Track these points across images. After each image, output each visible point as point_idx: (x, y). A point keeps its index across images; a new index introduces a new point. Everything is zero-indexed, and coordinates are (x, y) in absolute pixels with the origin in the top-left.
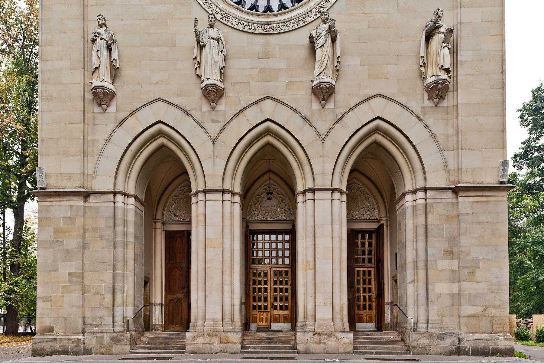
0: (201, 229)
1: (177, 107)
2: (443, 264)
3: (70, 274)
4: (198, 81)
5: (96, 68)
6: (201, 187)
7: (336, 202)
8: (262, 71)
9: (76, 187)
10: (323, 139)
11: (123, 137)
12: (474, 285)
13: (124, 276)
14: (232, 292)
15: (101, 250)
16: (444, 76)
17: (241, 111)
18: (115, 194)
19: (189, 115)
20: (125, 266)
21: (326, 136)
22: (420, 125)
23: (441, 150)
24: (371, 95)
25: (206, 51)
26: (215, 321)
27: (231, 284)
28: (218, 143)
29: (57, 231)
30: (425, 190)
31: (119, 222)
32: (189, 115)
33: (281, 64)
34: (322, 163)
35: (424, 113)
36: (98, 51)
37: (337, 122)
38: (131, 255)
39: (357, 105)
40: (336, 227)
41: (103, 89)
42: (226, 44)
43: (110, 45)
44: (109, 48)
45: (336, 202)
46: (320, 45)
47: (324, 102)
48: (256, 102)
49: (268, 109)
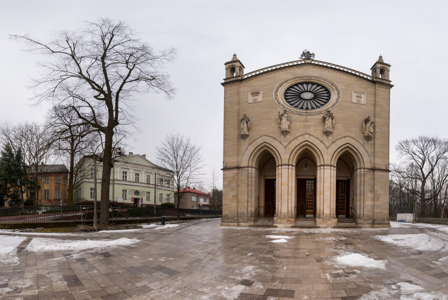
0: (280, 179)
1: (271, 137)
3: (233, 196)
4: (279, 129)
6: (280, 163)
7: (332, 170)
8: (304, 126)
11: (251, 148)
12: (378, 202)
14: (292, 203)
15: (243, 188)
18: (248, 167)
20: (252, 193)
27: (291, 199)
31: (250, 177)
33: (312, 124)
37: (333, 143)
38: (253, 189)
39: (340, 138)
40: (332, 179)
45: (332, 170)
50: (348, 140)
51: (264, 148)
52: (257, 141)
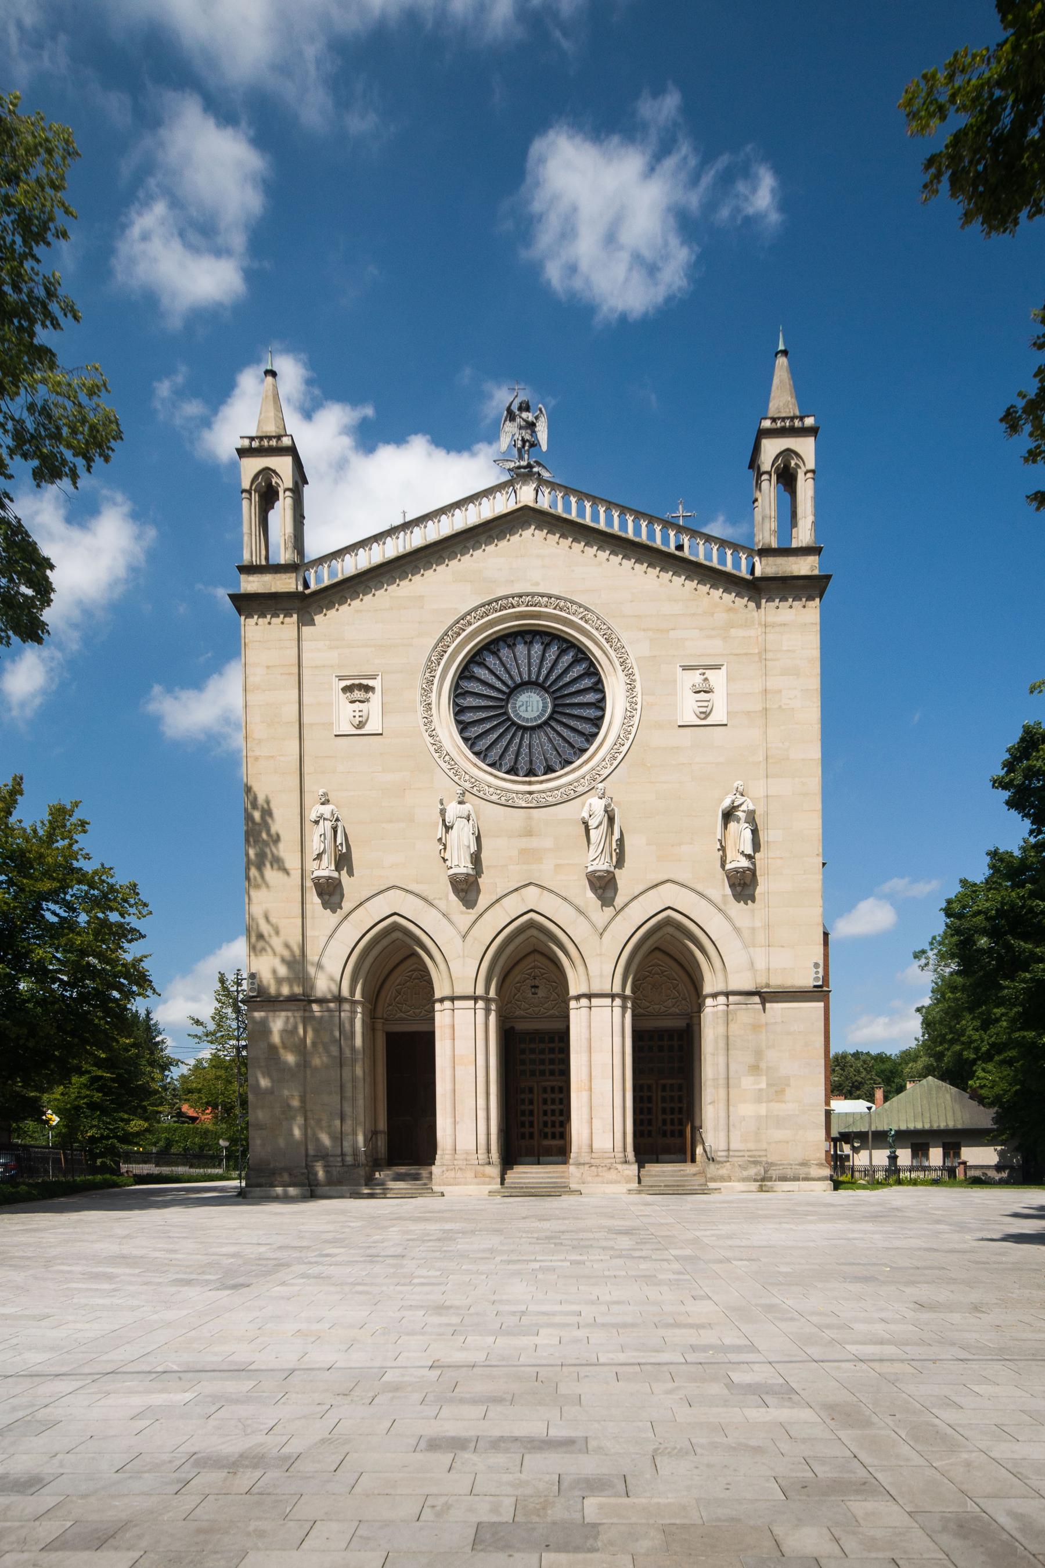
1: (417, 895)
2: (748, 1083)
8: (523, 852)
13: (354, 1099)
16: (744, 863)
17: (498, 901)
20: (354, 1087)
22: (720, 917)
23: (746, 947)
25: (453, 833)
30: (727, 994)
34: (597, 961)
35: (725, 903)
48: (516, 890)
49: (532, 898)
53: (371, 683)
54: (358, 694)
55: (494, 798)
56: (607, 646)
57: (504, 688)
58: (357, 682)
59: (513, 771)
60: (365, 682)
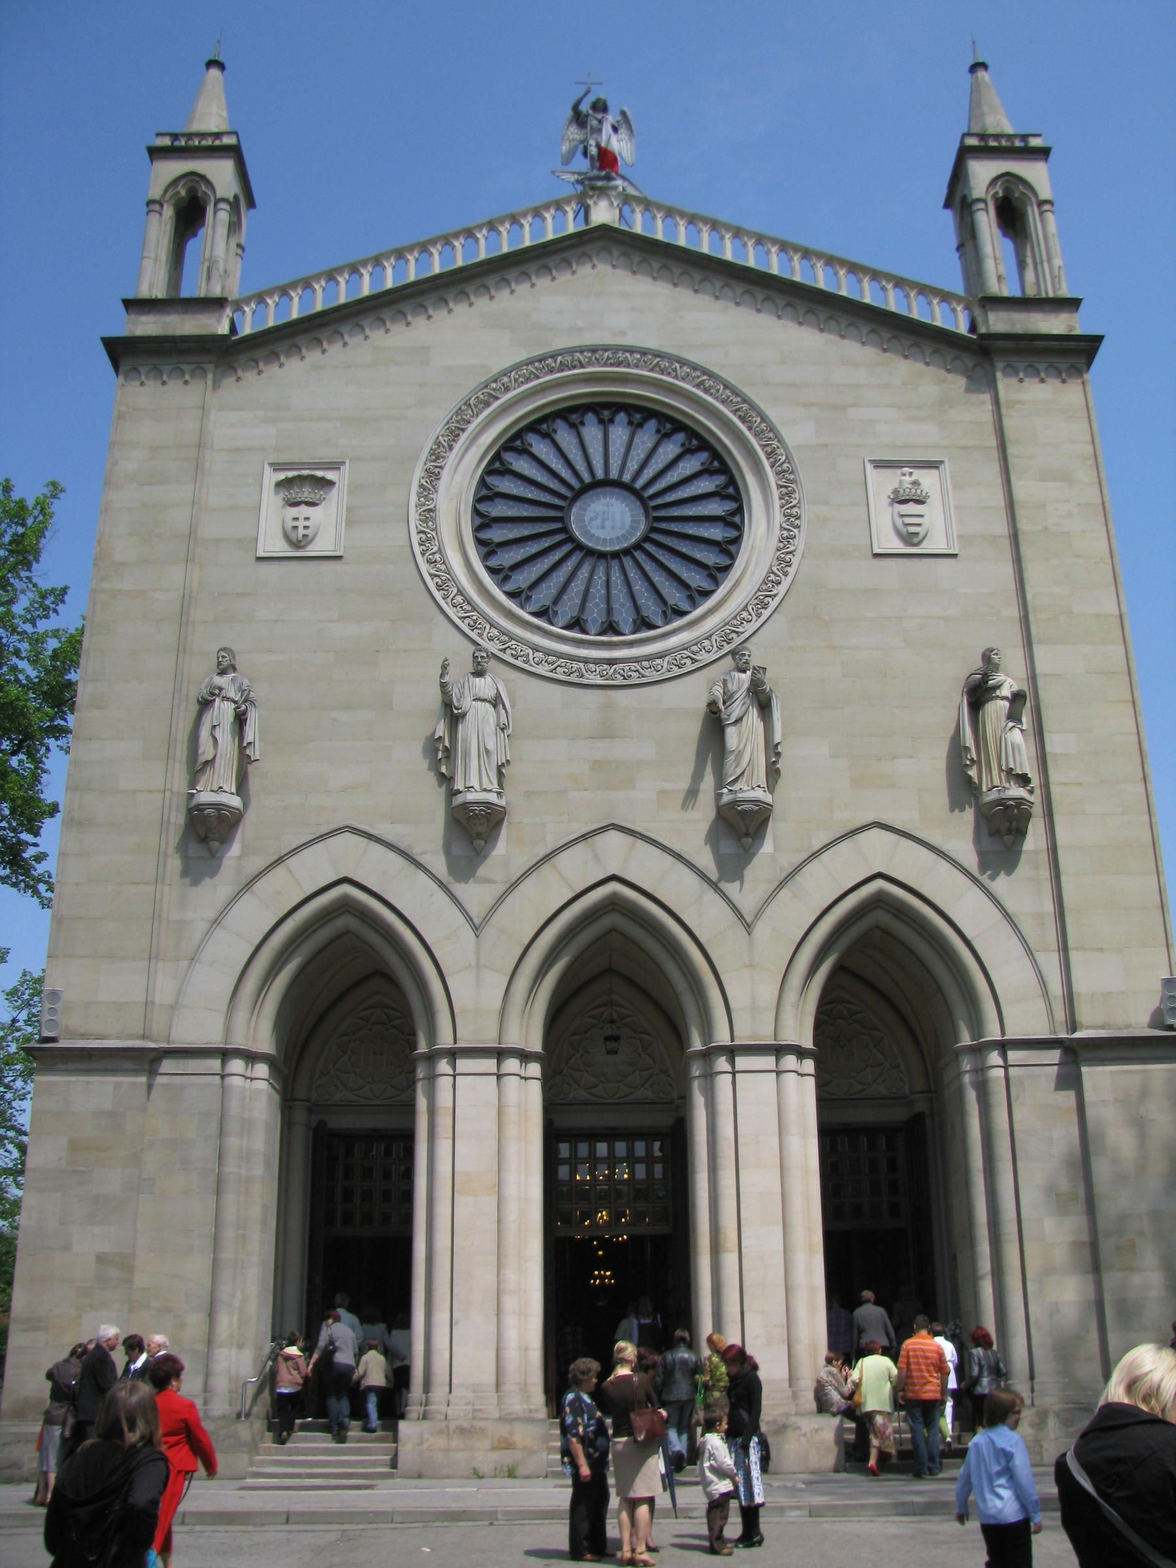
5: (207, 763)
8: (597, 765)
9: (131, 1037)
10: (749, 927)
11: (255, 916)
17: (548, 857)
19: (419, 865)
21: (757, 916)
24: (858, 824)
26: (476, 1389)
28: (489, 932)
29: (75, 1146)
31: (233, 1125)
32: (419, 865)
36: (214, 727)
37: (781, 885)
38: (255, 1212)
41: (219, 810)
42: (512, 706)
43: (245, 712)
44: (240, 720)
46: (733, 719)
47: (750, 840)
48: (584, 837)
49: (616, 854)
50: (878, 853)
51: (341, 923)
52: (292, 862)
53: (330, 475)
54: (306, 493)
55: (542, 670)
56: (743, 428)
57: (563, 490)
58: (305, 473)
59: (576, 624)
60: (319, 474)
